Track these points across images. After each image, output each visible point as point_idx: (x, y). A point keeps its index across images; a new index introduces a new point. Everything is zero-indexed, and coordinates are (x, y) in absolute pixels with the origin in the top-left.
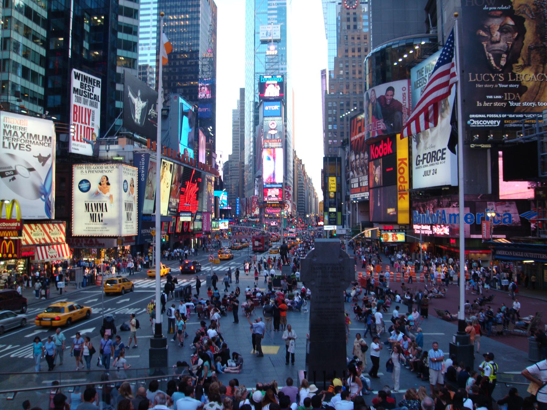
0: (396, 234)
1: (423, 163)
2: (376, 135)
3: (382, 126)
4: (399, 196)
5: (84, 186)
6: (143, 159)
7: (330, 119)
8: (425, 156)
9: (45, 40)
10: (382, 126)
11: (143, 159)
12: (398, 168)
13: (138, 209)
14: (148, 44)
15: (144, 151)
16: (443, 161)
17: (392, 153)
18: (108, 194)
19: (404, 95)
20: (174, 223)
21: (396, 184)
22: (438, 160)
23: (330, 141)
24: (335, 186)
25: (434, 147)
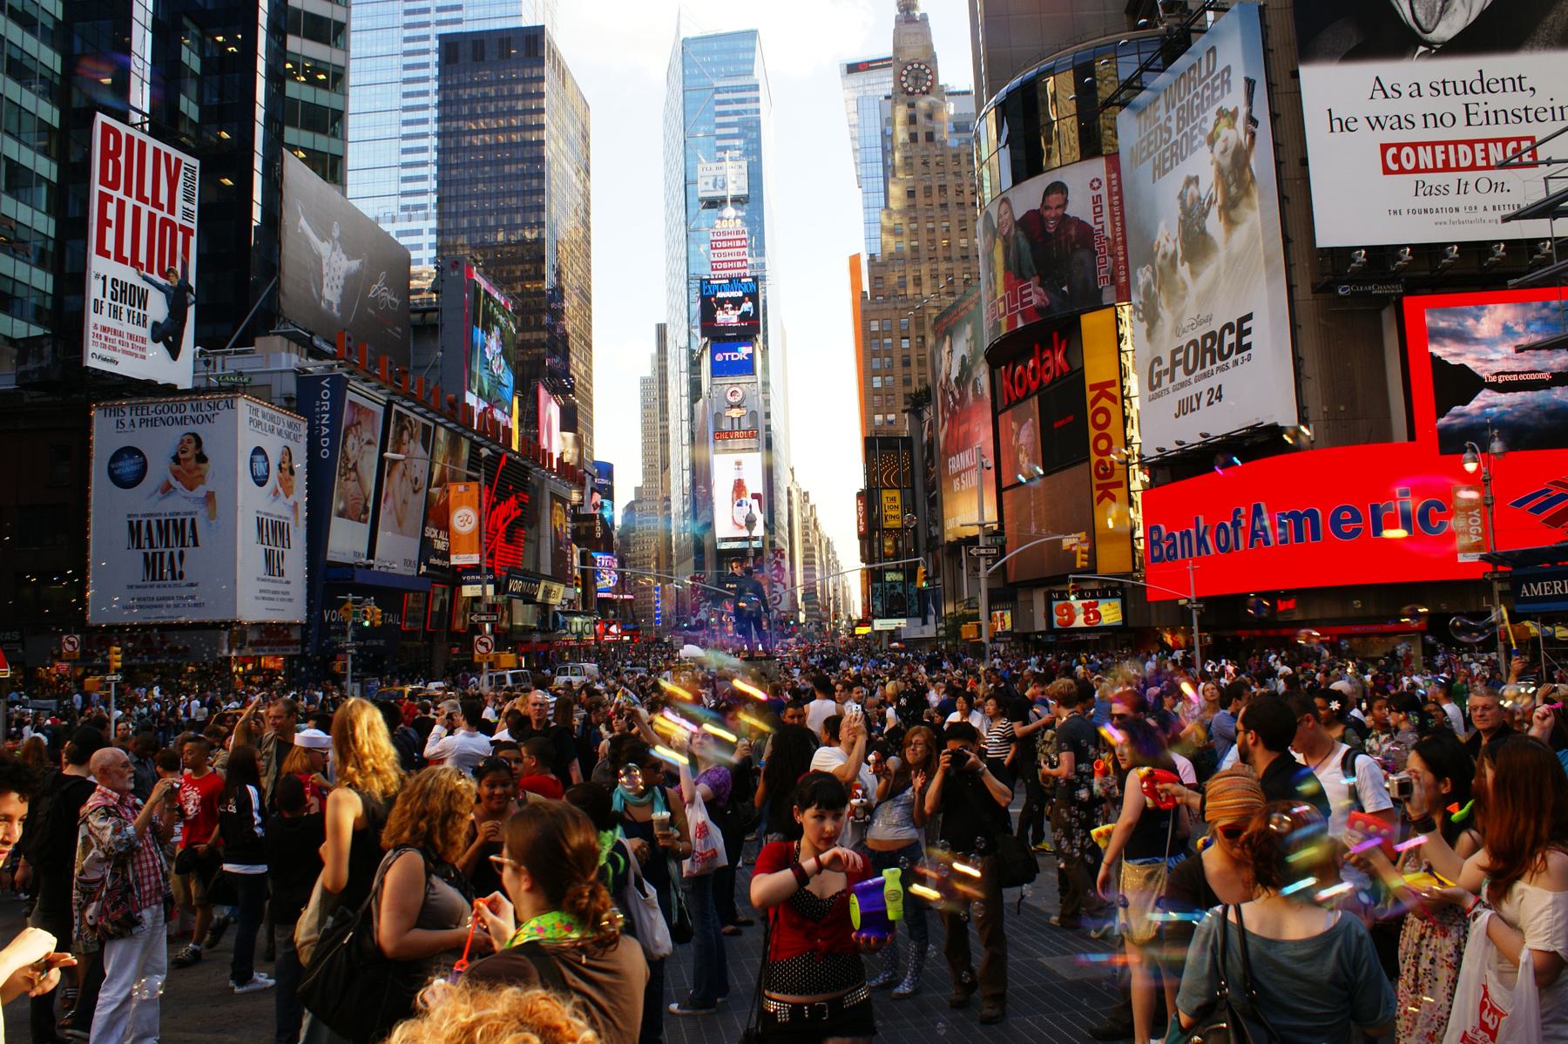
0: (1096, 604)
1: (1172, 379)
2: (1020, 324)
3: (1036, 296)
4: (1097, 494)
5: (127, 467)
6: (326, 394)
7: (876, 363)
8: (1180, 356)
9: (57, 81)
10: (1036, 296)
11: (326, 394)
12: (1090, 412)
13: (309, 549)
14: (424, 207)
15: (331, 368)
16: (1245, 354)
17: (1071, 372)
18: (200, 491)
19: (1097, 200)
20: (443, 603)
21: (1088, 459)
22: (1223, 358)
23: (879, 418)
24: (897, 512)
25: (1209, 319)
